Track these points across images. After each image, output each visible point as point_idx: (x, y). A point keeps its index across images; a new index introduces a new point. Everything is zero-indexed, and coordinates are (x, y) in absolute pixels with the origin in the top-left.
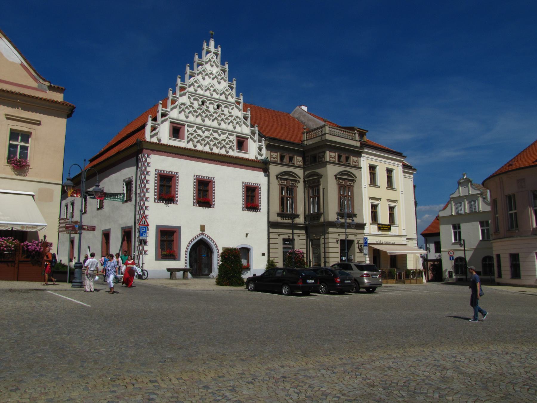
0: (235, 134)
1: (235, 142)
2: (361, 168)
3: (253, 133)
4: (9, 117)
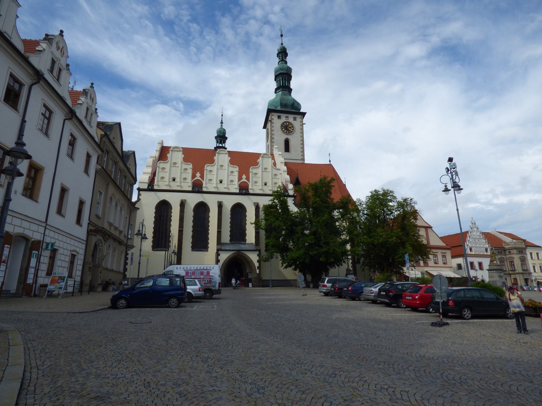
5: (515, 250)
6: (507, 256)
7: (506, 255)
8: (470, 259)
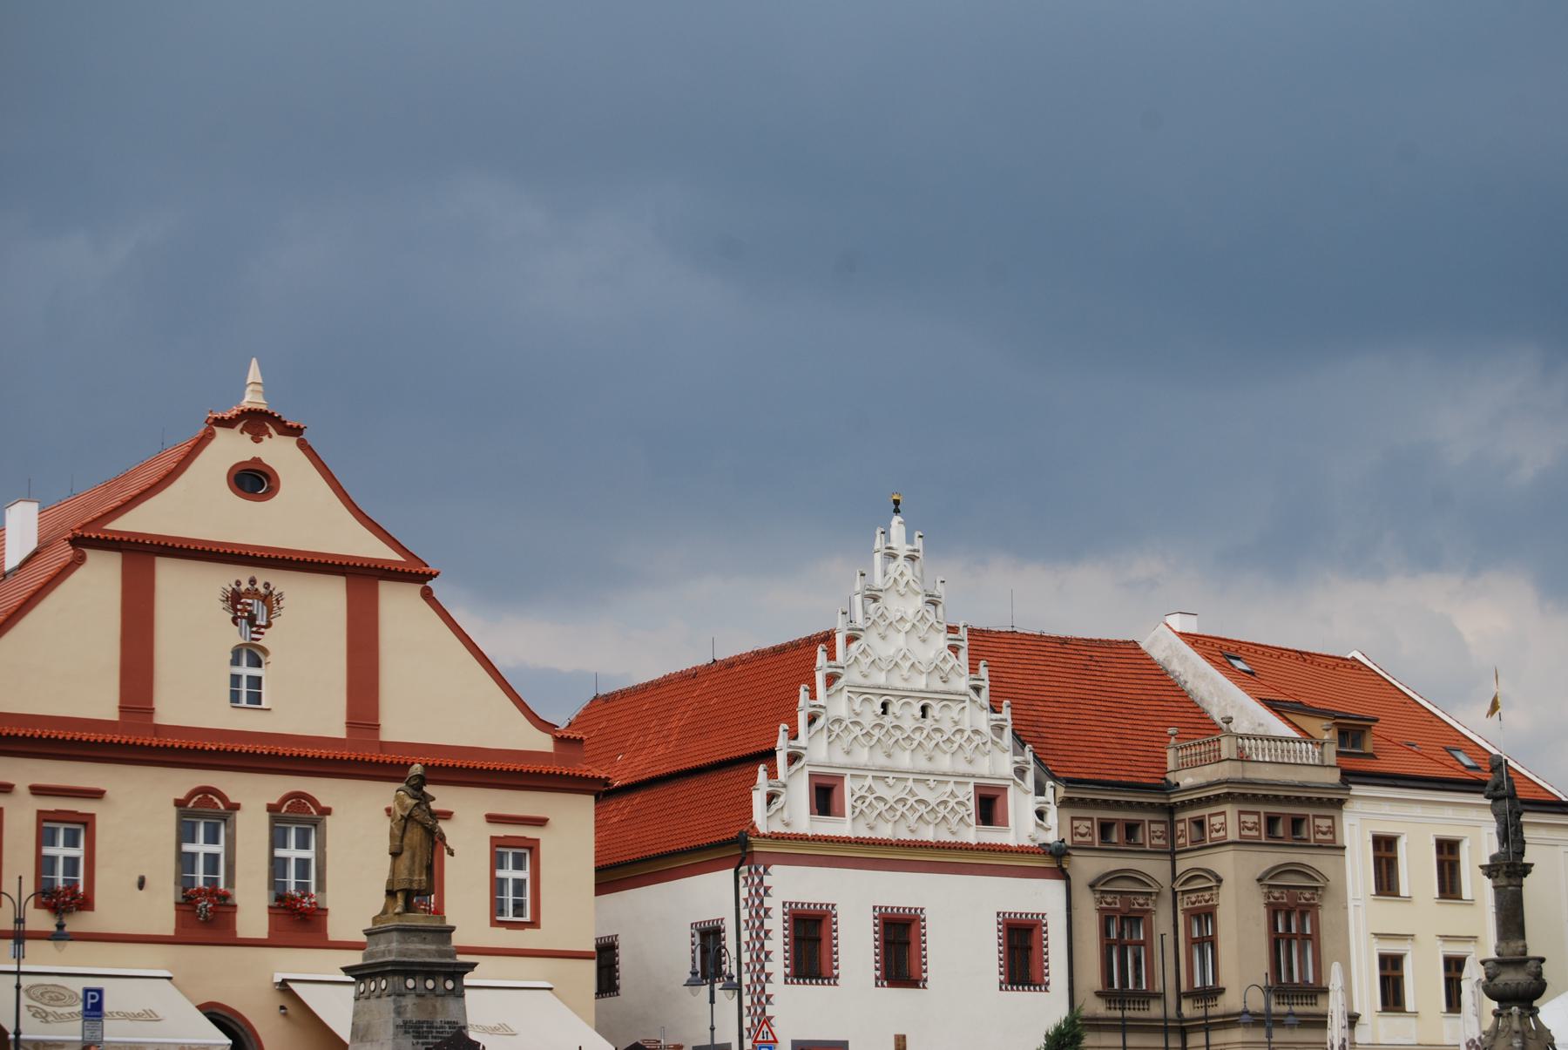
0: (972, 781)
1: (972, 805)
2: (1344, 848)
3: (1020, 772)
4: (492, 819)
5: (1231, 810)
6: (1184, 864)
7: (1172, 854)
8: (791, 885)
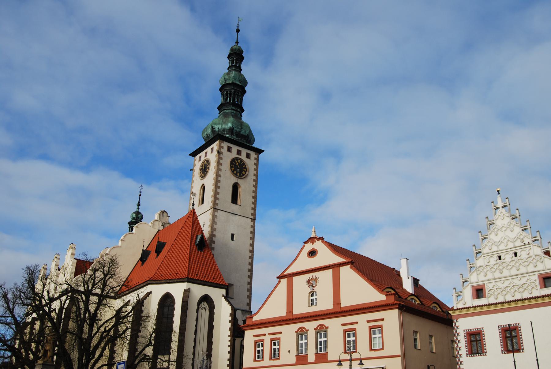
0: (536, 273)
